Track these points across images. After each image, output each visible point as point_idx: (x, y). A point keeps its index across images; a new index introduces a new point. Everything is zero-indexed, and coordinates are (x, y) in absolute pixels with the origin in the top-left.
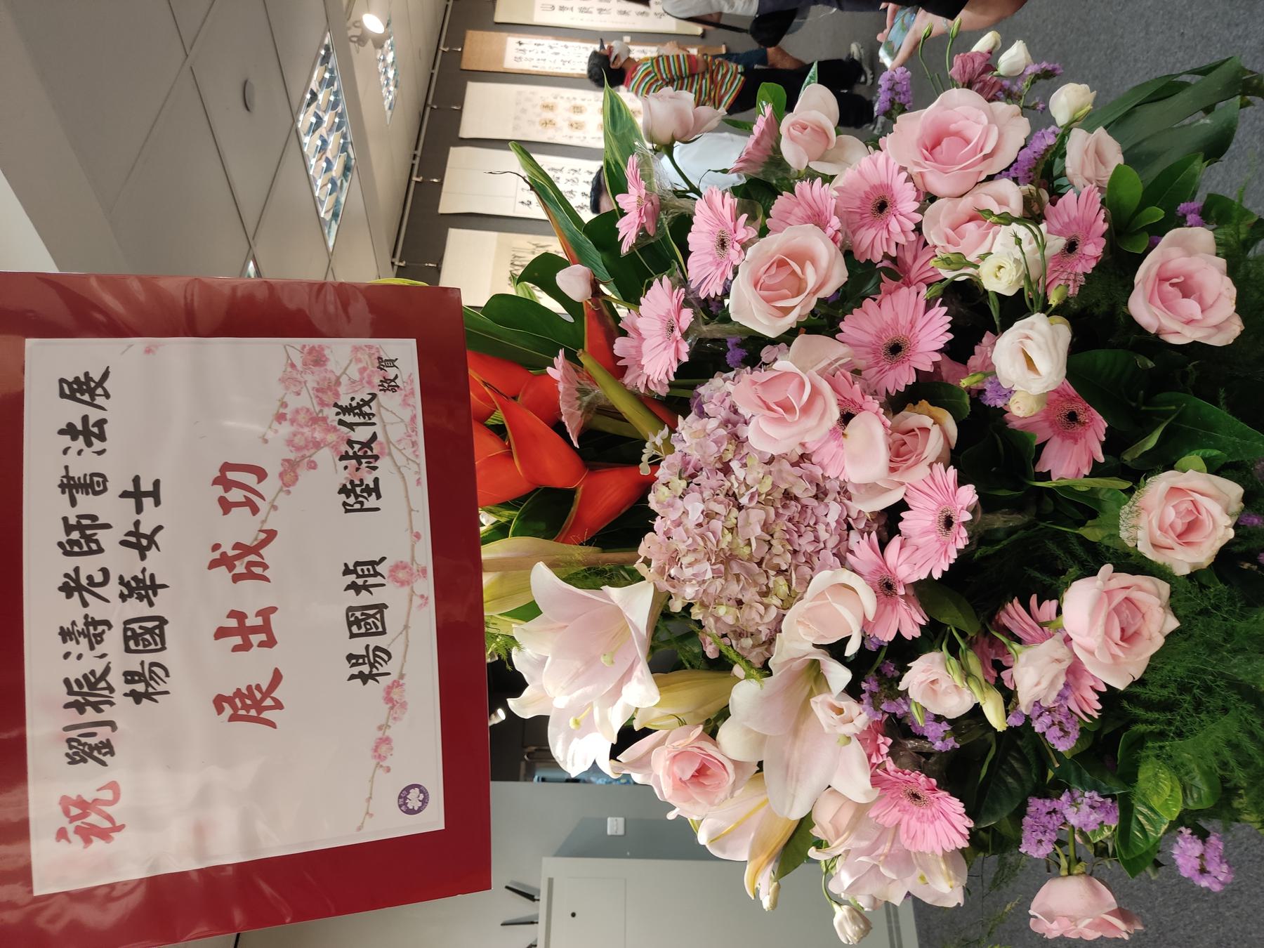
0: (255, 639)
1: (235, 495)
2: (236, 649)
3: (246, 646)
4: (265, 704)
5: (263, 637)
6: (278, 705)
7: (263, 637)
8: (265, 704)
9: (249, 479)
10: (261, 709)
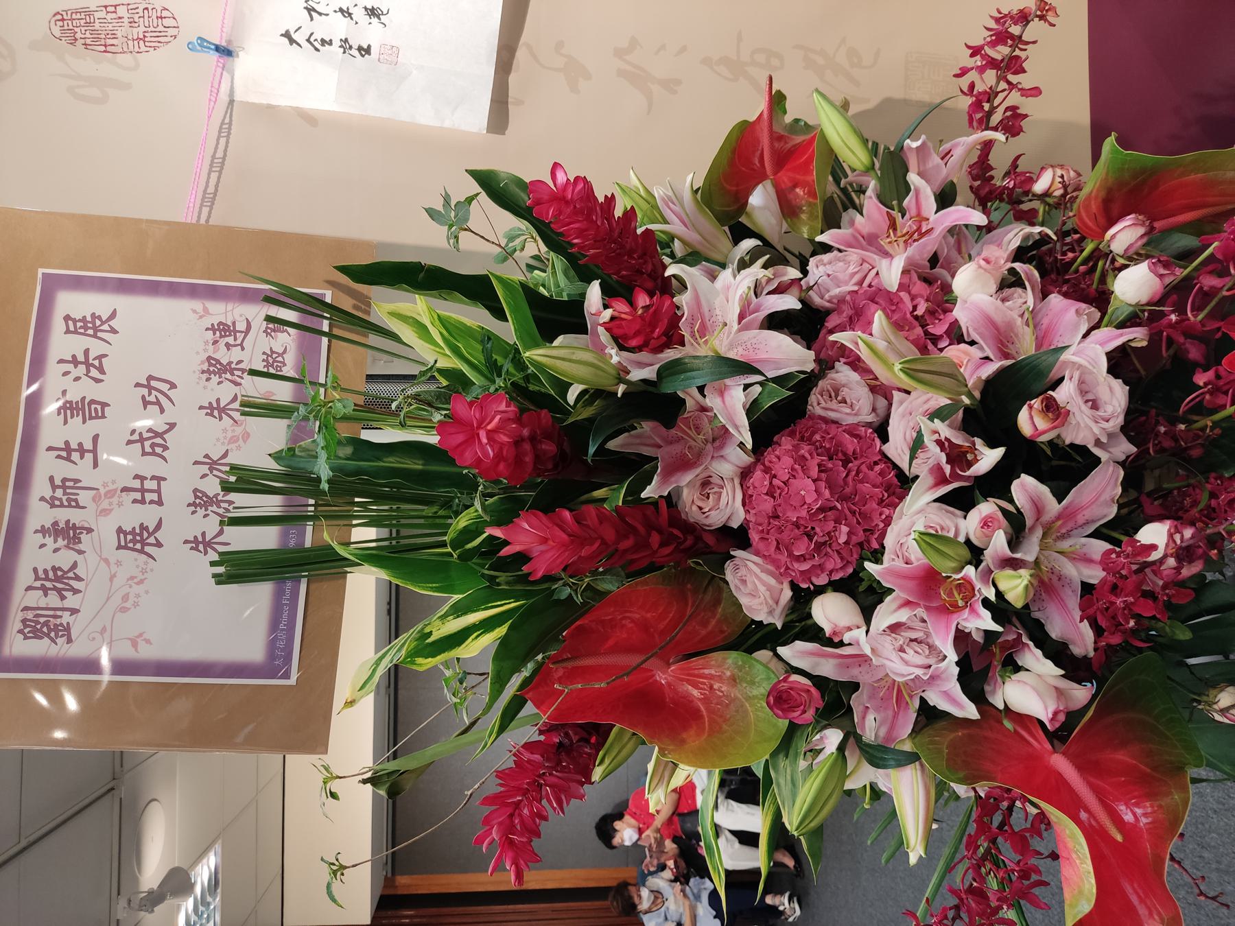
0: (149, 497)
1: (152, 399)
2: (135, 501)
3: (143, 501)
4: (148, 541)
5: (155, 497)
6: (159, 544)
7: (155, 497)
8: (148, 541)
9: (164, 387)
10: (144, 543)
